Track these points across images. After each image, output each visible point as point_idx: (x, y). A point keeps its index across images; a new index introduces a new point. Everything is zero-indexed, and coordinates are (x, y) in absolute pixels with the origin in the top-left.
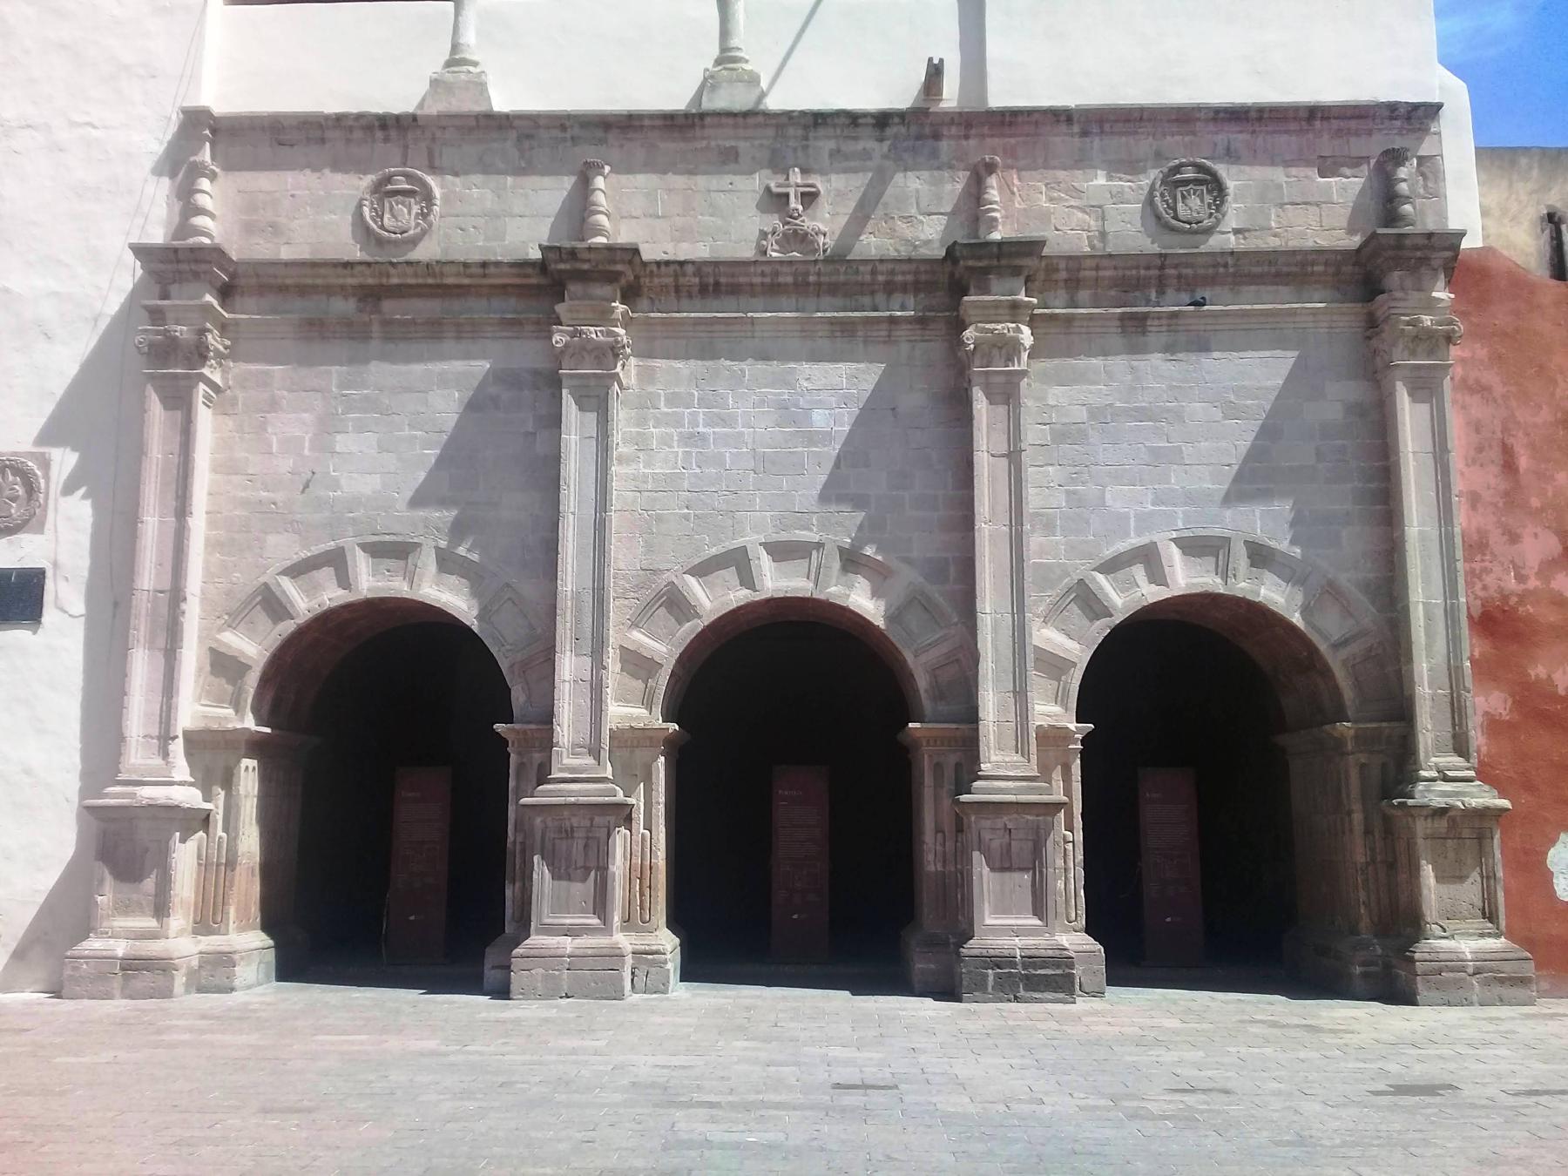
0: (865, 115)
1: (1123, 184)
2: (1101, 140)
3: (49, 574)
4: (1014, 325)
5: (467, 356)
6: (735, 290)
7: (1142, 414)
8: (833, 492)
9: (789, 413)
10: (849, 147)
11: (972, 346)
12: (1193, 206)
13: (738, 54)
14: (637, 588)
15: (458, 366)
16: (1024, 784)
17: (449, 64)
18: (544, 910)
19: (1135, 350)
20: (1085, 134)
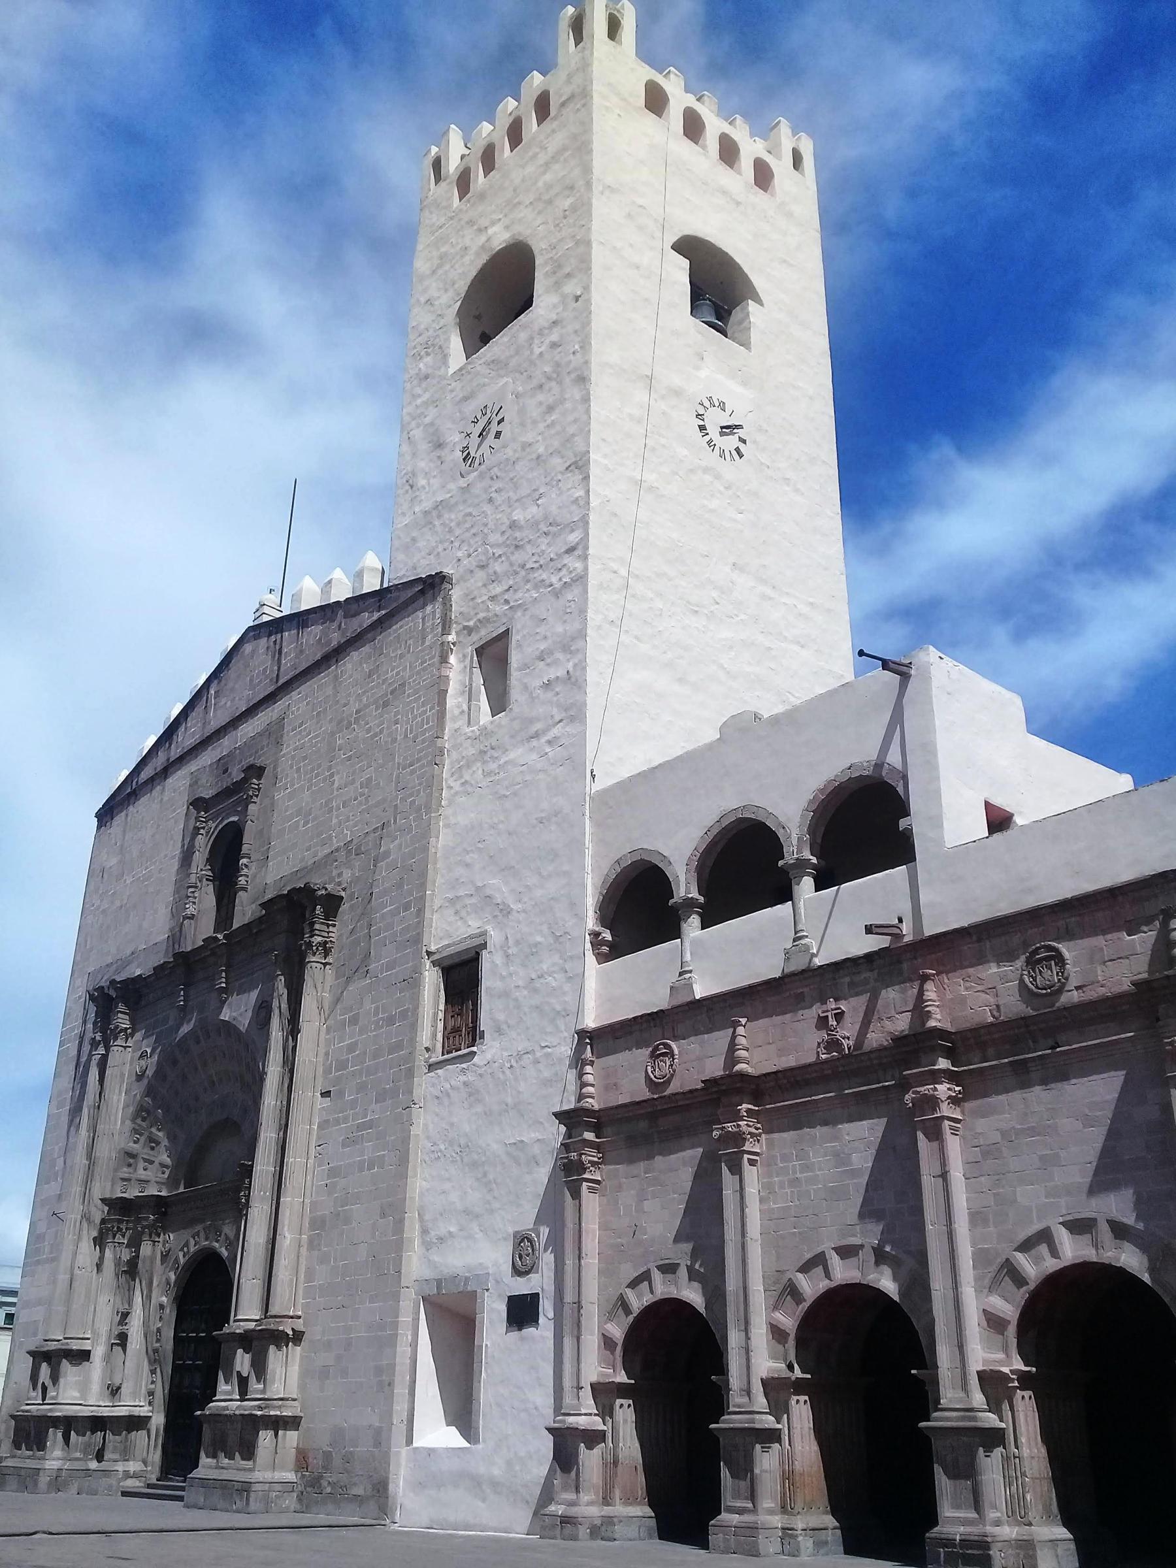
0: (860, 958)
1: (1006, 968)
2: (990, 942)
3: (541, 1296)
4: (932, 1086)
5: (693, 1147)
6: (807, 1083)
7: (1032, 1131)
8: (868, 1212)
9: (841, 1159)
10: (857, 979)
11: (911, 1105)
12: (1050, 975)
13: (805, 934)
14: (775, 1283)
15: (689, 1153)
16: (962, 1414)
17: (681, 974)
18: (727, 1500)
19: (1025, 1085)
20: (979, 940)
